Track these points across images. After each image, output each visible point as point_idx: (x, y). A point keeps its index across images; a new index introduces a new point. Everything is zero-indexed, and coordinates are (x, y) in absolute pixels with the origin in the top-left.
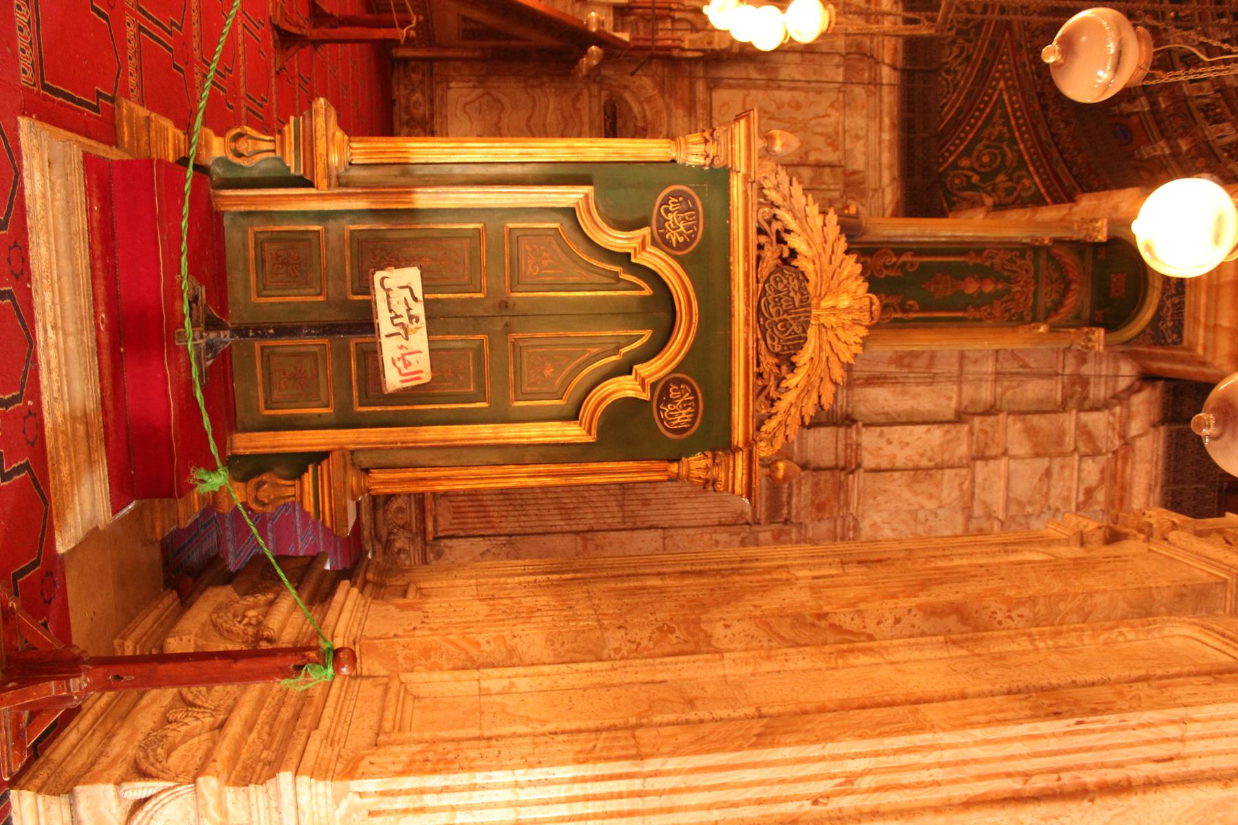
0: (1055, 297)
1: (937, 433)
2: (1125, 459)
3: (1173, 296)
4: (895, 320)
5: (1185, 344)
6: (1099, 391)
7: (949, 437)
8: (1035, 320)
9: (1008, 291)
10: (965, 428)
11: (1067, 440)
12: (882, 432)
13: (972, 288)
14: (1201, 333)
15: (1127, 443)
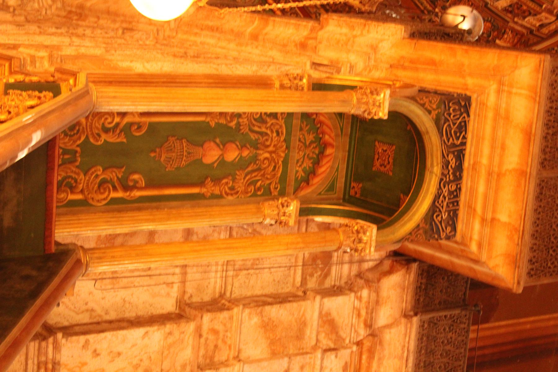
0: (308, 164)
1: (156, 336)
2: (371, 352)
3: (450, 182)
4: (114, 201)
5: (458, 237)
6: (341, 271)
7: (170, 340)
8: (282, 193)
9: (255, 159)
10: (191, 327)
11: (308, 332)
12: (87, 342)
13: (212, 155)
14: (477, 226)
15: (374, 334)
